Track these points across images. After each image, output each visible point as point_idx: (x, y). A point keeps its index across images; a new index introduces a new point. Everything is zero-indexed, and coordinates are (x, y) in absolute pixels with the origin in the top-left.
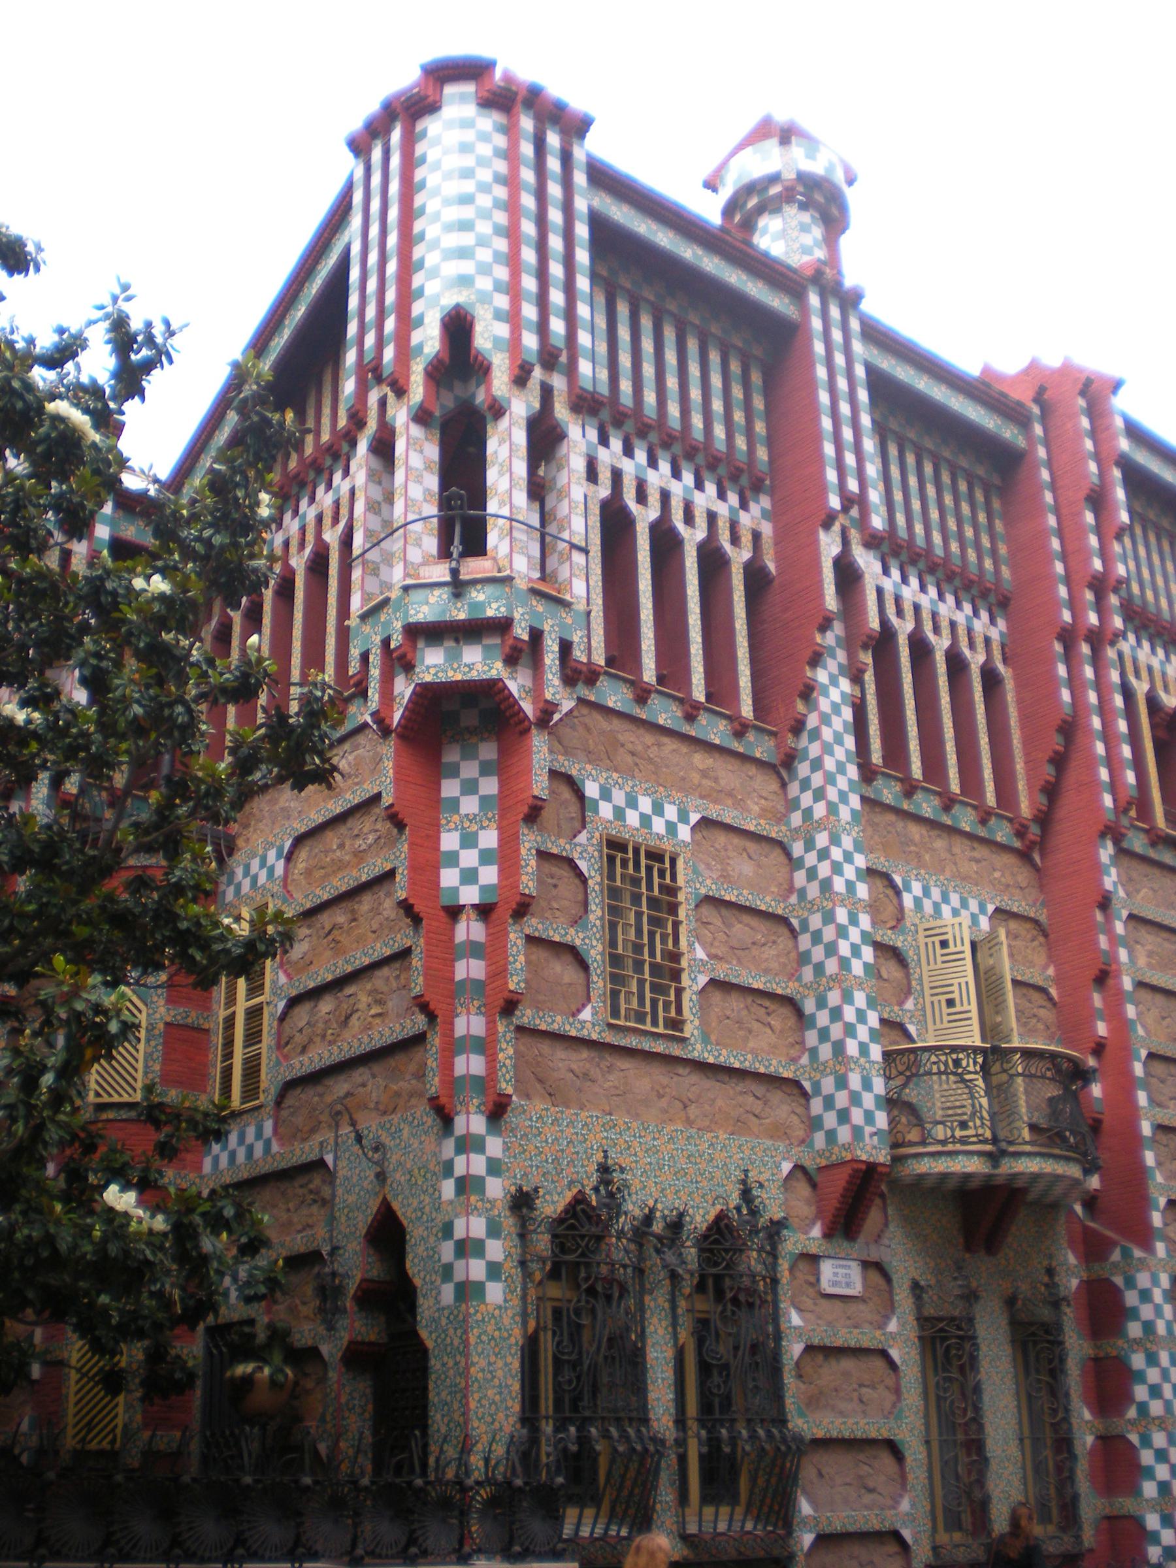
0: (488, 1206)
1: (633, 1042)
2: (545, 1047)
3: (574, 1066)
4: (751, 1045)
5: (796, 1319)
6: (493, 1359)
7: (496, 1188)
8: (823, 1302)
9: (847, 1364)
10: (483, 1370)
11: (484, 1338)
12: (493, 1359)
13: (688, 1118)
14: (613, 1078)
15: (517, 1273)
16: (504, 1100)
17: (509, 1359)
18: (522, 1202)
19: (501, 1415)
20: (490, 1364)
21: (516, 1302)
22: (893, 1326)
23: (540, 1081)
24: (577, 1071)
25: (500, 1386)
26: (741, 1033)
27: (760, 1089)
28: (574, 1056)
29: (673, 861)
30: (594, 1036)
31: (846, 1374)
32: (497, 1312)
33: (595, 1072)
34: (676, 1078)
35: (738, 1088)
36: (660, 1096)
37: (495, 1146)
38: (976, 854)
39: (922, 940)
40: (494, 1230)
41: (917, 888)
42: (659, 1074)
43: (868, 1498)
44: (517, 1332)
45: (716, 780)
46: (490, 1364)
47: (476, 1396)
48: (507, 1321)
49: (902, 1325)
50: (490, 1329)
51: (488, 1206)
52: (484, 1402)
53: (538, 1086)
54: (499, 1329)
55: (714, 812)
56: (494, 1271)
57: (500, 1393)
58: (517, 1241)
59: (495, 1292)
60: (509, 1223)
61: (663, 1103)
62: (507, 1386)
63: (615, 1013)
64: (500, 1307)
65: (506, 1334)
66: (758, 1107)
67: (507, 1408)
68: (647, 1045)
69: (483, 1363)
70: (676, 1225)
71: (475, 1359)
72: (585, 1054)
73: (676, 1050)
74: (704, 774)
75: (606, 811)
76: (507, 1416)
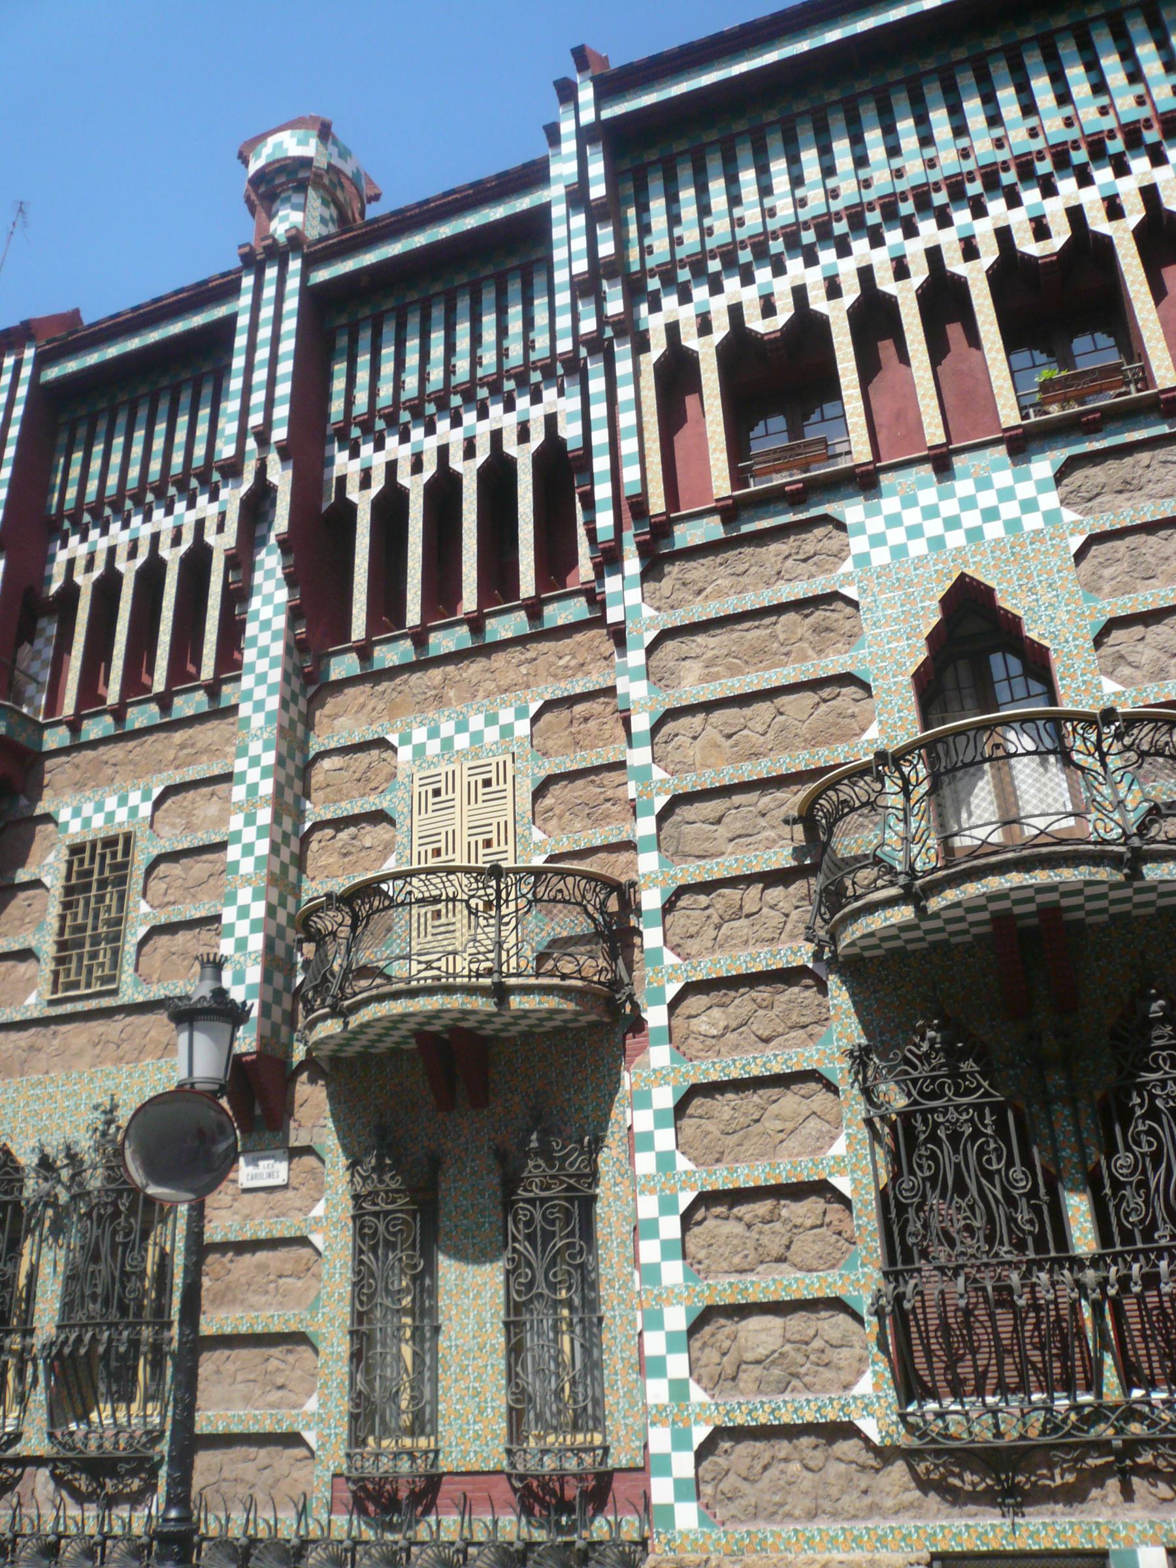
8: (247, 1197)
9: (262, 1256)
22: (319, 1210)
26: (186, 963)
29: (128, 838)
31: (262, 1267)
33: (40, 1042)
38: (529, 655)
39: (416, 790)
41: (419, 735)
42: (98, 1027)
43: (275, 1396)
45: (193, 745)
49: (332, 1206)
55: (177, 777)
68: (80, 1006)
73: (106, 1002)
74: (182, 746)
75: (75, 826)
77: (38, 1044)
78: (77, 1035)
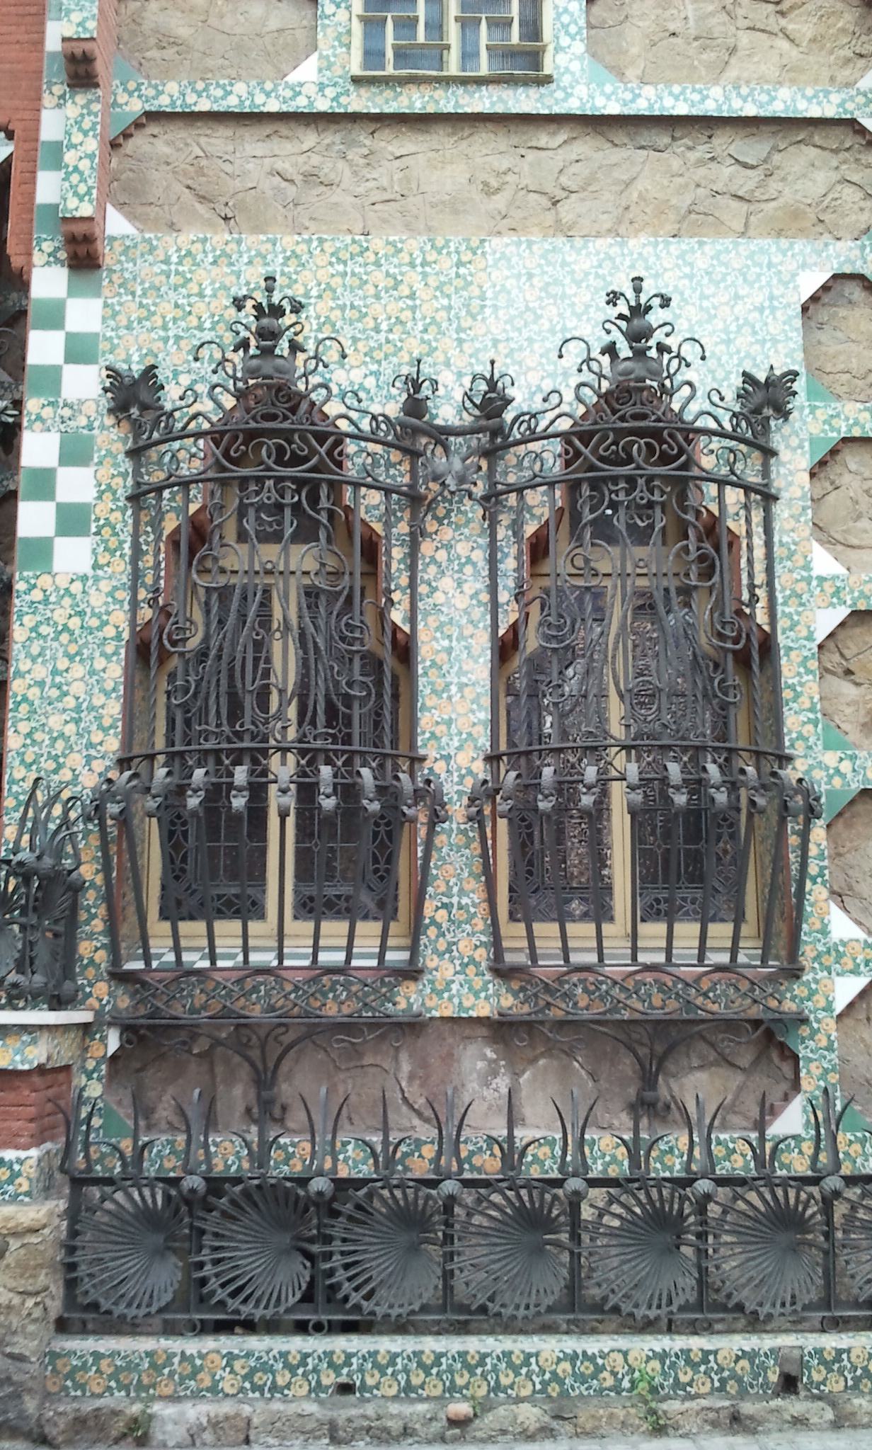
0: (67, 412)
1: (415, 100)
2: (218, 140)
3: (284, 166)
4: (732, 73)
5: (824, 562)
6: (63, 664)
7: (84, 385)
10: (41, 684)
11: (44, 630)
12: (63, 664)
13: (558, 221)
14: (385, 174)
15: (123, 520)
16: (79, 229)
17: (100, 663)
18: (133, 396)
19: (76, 760)
20: (55, 672)
21: (121, 568)
23: (203, 198)
24: (290, 171)
25: (78, 709)
27: (753, 149)
28: (277, 146)
30: (322, 106)
32: (76, 588)
33: (331, 167)
34: (531, 156)
35: (693, 156)
36: (489, 191)
37: (84, 314)
40: (75, 452)
42: (488, 150)
44: (120, 618)
46: (55, 672)
47: (24, 727)
48: (97, 600)
50: (59, 616)
51: (67, 412)
52: (38, 736)
53: (201, 209)
54: (81, 614)
56: (73, 520)
57: (78, 721)
58: (127, 465)
59: (73, 555)
60: (112, 439)
61: (500, 201)
62: (91, 708)
63: (372, 55)
64: (84, 578)
65: (95, 622)
66: (747, 182)
67: (90, 745)
69: (40, 672)
70: (491, 402)
71: (24, 665)
72: (309, 138)
76: (89, 759)
77: (326, 171)
78: (441, 165)
